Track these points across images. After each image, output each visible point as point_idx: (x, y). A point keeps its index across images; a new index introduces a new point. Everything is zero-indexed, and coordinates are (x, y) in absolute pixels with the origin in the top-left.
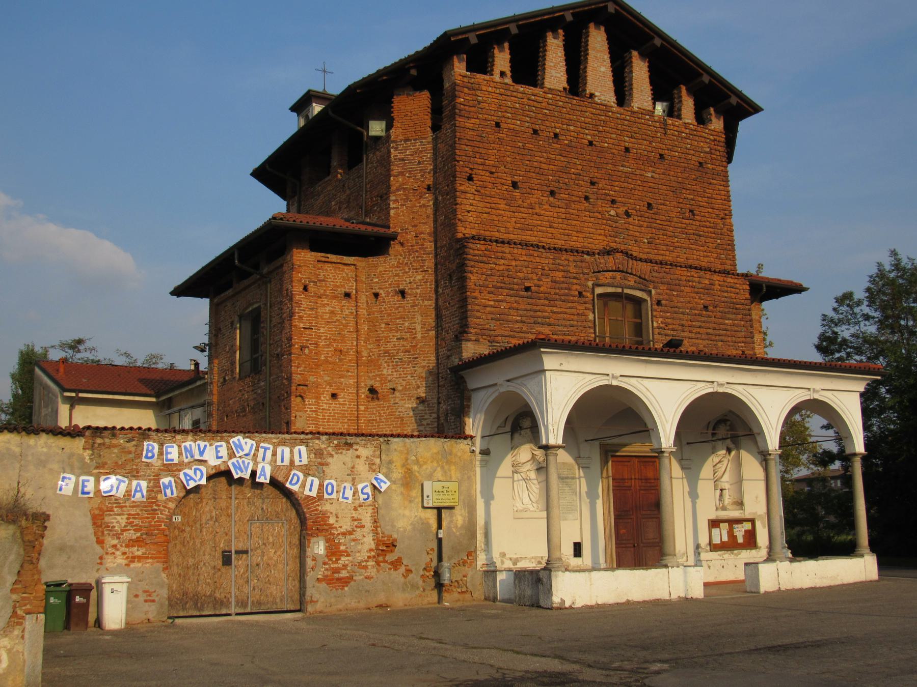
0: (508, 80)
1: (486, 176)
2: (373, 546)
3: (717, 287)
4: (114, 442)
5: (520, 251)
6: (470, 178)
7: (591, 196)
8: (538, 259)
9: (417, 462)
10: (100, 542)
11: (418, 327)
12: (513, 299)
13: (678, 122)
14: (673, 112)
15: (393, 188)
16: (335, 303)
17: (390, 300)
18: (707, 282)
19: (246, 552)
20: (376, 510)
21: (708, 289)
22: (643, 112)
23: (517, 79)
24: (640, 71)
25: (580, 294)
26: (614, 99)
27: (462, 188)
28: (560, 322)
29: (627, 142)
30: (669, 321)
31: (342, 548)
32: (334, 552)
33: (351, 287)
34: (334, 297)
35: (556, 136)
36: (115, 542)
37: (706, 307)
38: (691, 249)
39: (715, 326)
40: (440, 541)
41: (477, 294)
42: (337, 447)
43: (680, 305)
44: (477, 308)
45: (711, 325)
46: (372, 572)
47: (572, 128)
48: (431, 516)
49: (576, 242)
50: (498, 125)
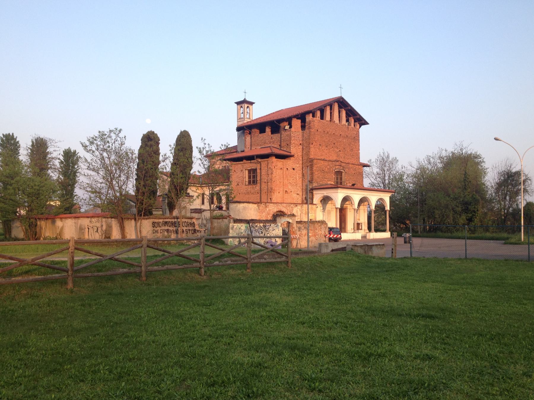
24: (344, 113)
33: (282, 167)
49: (331, 158)
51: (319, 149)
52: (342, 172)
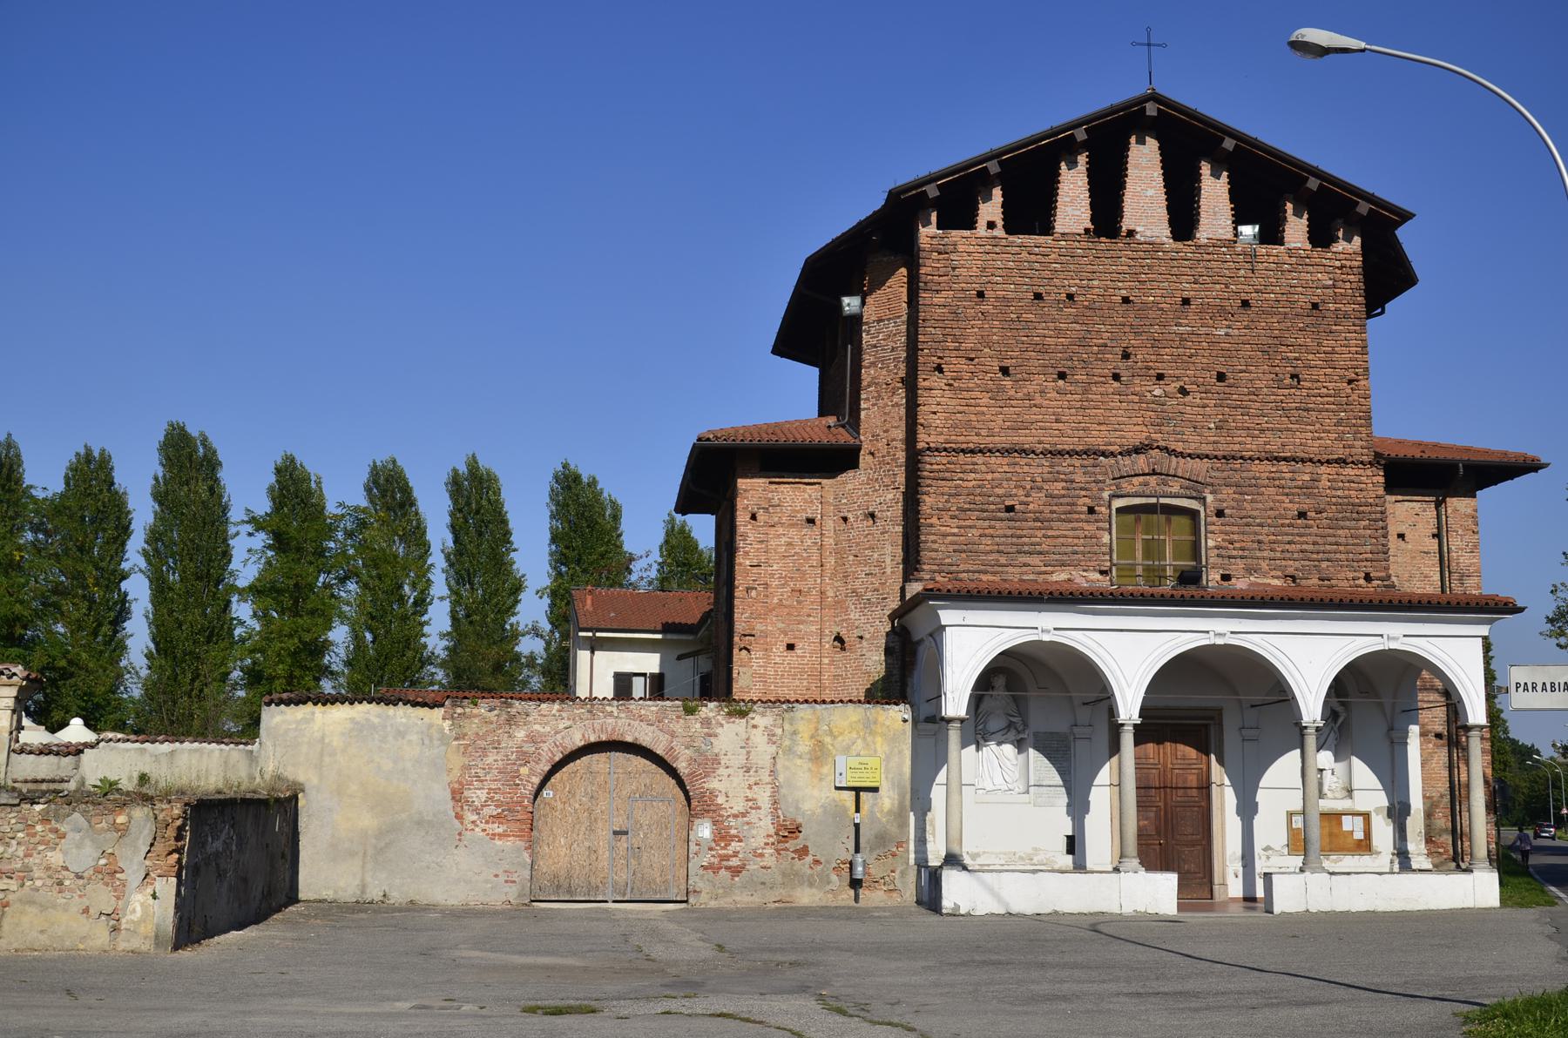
0: (999, 232)
1: (963, 365)
2: (772, 831)
3: (1325, 483)
4: (475, 711)
5: (1000, 460)
6: (939, 369)
7: (1123, 373)
8: (1026, 469)
9: (831, 733)
10: (459, 817)
11: (888, 560)
12: (987, 523)
13: (1276, 249)
14: (1272, 234)
15: (864, 383)
16: (793, 532)
17: (860, 526)
18: (1307, 477)
19: (626, 833)
20: (776, 789)
21: (1308, 489)
22: (1217, 244)
23: (1010, 228)
25: (1091, 510)
26: (1168, 232)
27: (926, 384)
28: (1057, 550)
29: (1187, 289)
30: (1236, 537)
31: (733, 832)
32: (722, 836)
33: (814, 511)
34: (792, 525)
35: (1070, 297)
36: (475, 817)
37: (1302, 515)
38: (1288, 430)
39: (1318, 539)
40: (857, 826)
41: (934, 520)
42: (730, 714)
43: (1255, 513)
44: (932, 538)
45: (1310, 539)
46: (770, 860)
47: (1096, 283)
48: (849, 797)
49: (1097, 438)
50: (981, 295)
51: (996, 393)
52: (1193, 514)
